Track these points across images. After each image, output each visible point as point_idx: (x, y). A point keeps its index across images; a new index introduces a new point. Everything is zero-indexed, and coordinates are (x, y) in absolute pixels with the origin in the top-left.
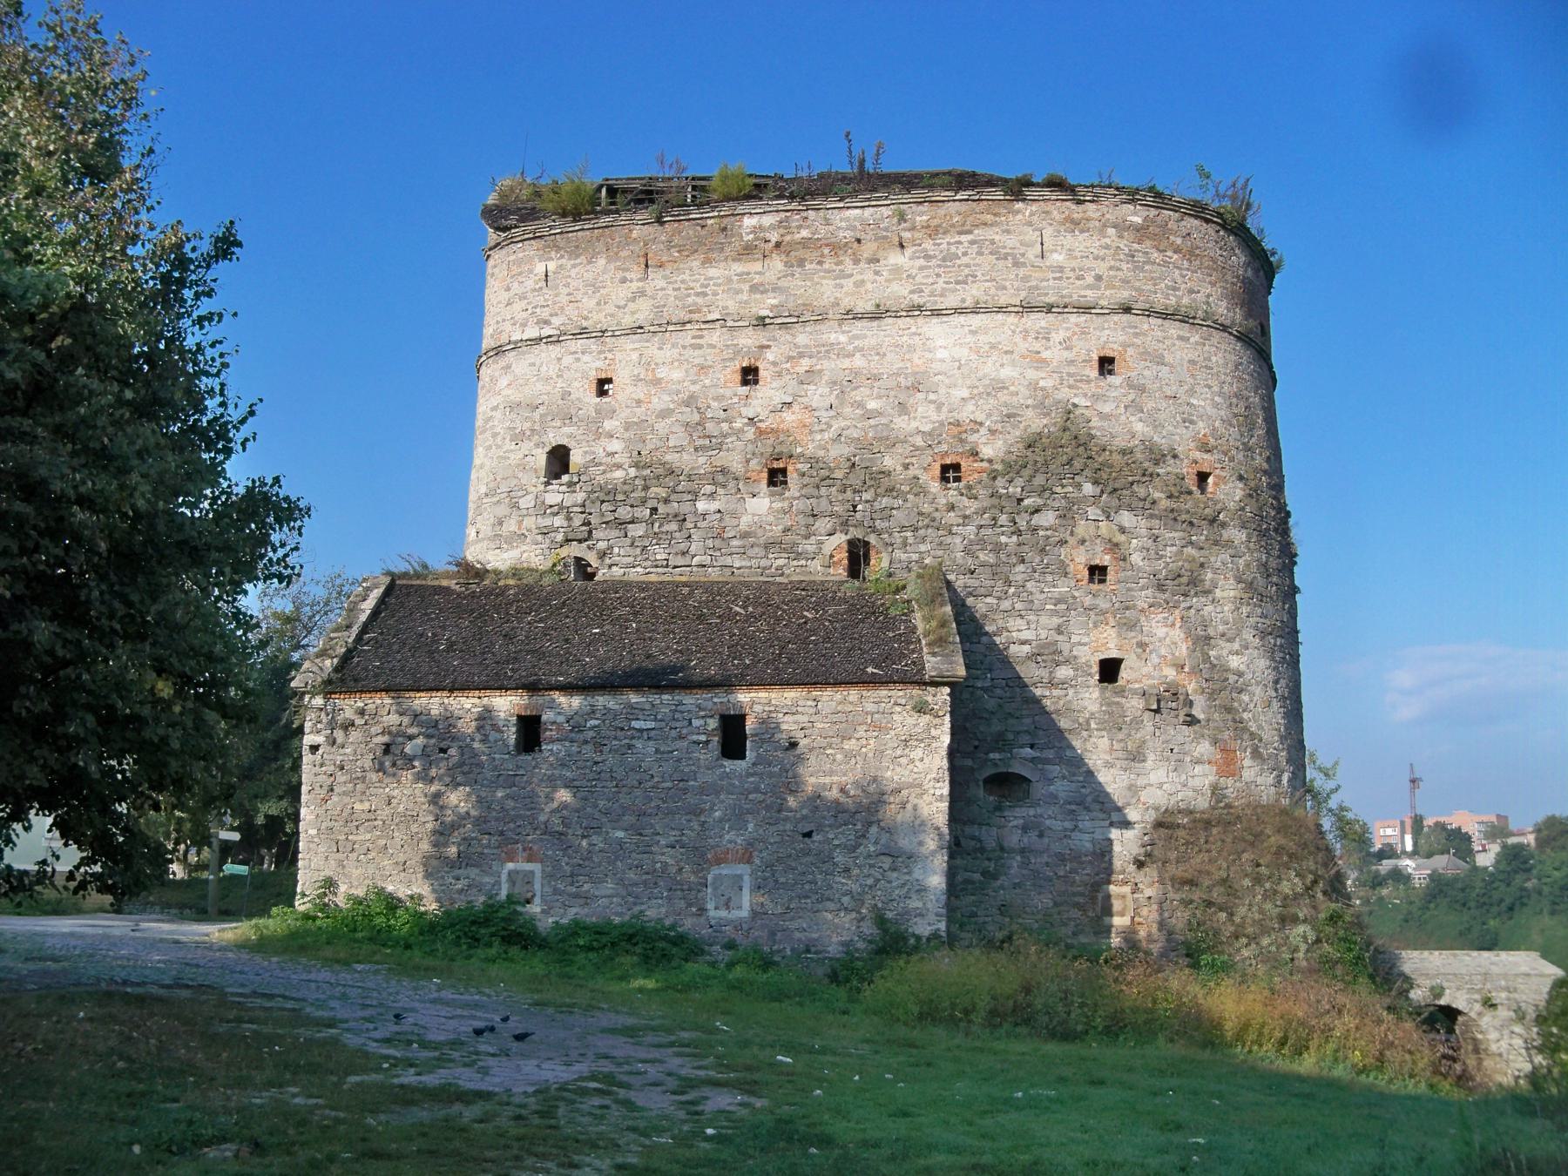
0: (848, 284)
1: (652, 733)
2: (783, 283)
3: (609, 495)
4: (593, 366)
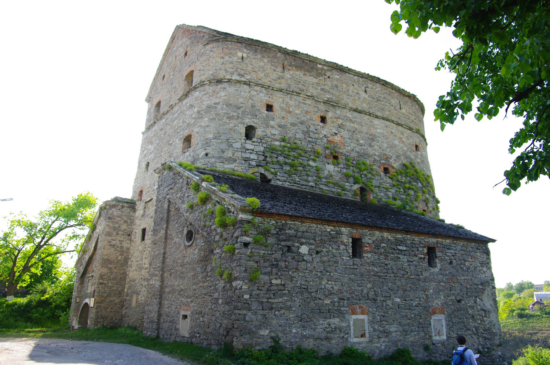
1: (406, 252)
2: (331, 91)
3: (273, 150)
4: (262, 98)
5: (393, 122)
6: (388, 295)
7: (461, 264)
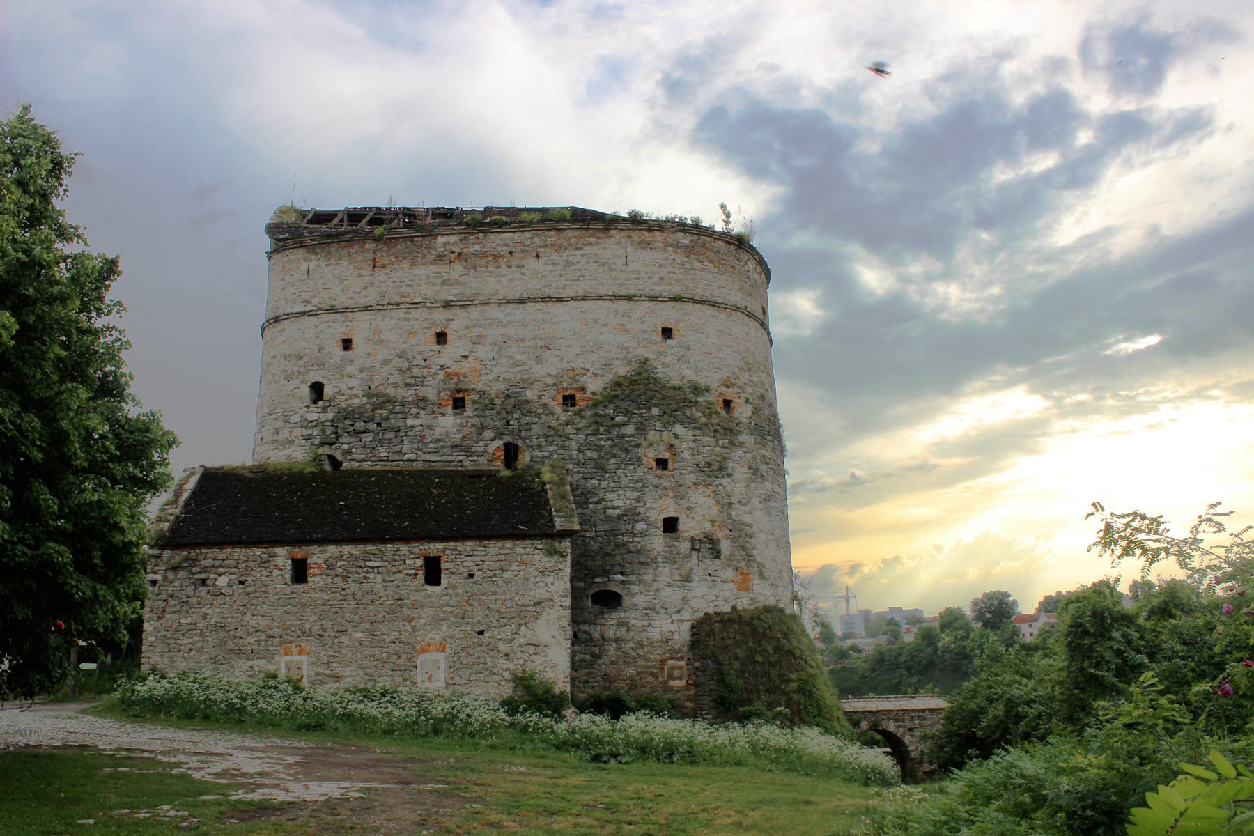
0: (505, 280)
3: (348, 414)
5: (600, 298)
6: (342, 629)
7: (495, 576)
